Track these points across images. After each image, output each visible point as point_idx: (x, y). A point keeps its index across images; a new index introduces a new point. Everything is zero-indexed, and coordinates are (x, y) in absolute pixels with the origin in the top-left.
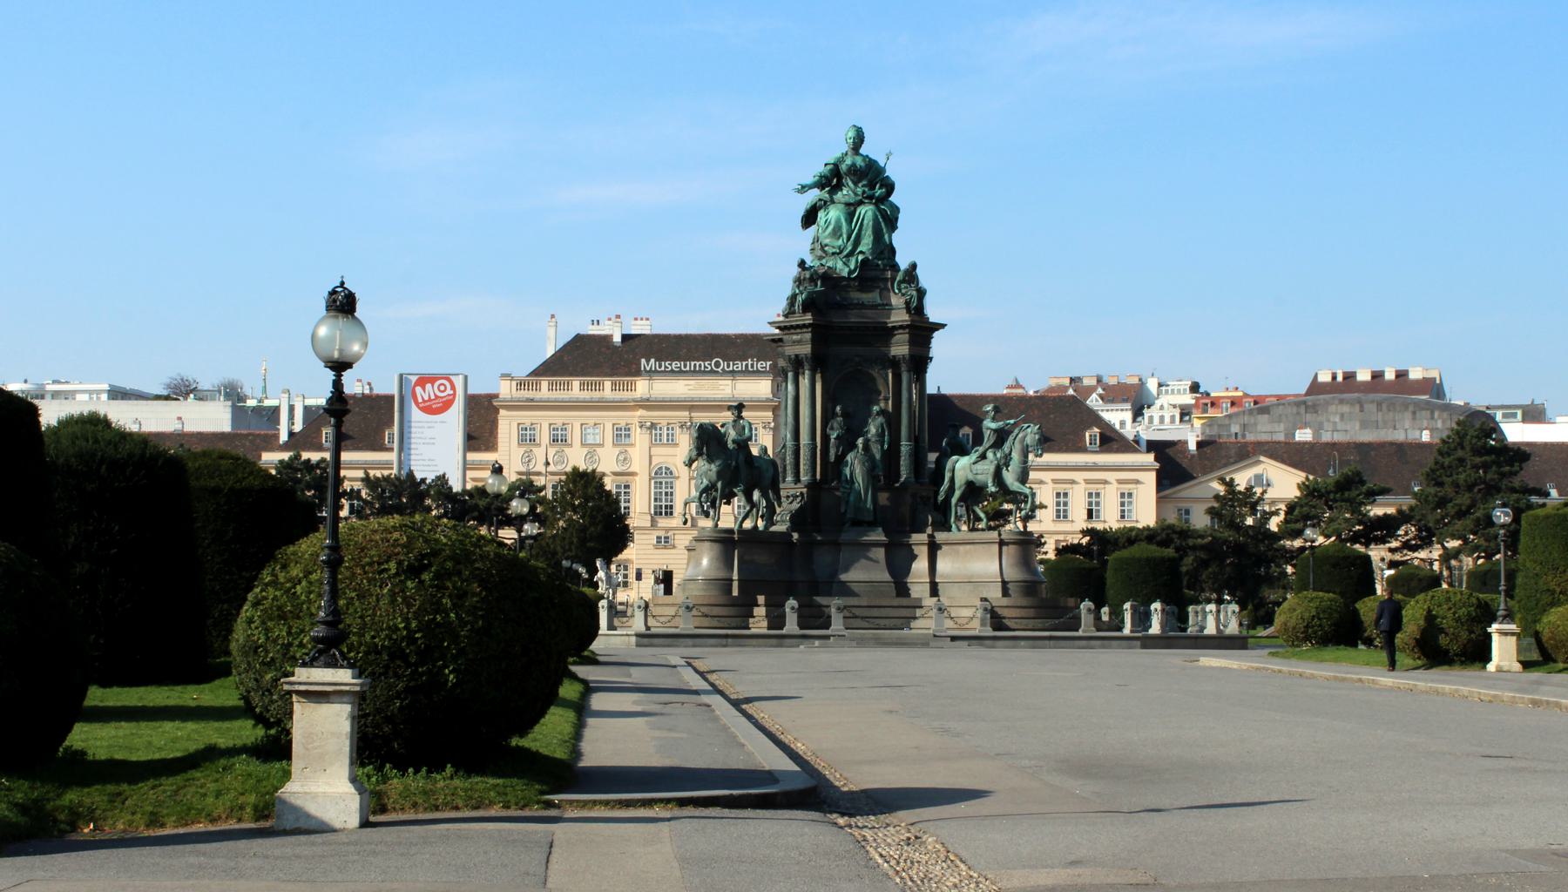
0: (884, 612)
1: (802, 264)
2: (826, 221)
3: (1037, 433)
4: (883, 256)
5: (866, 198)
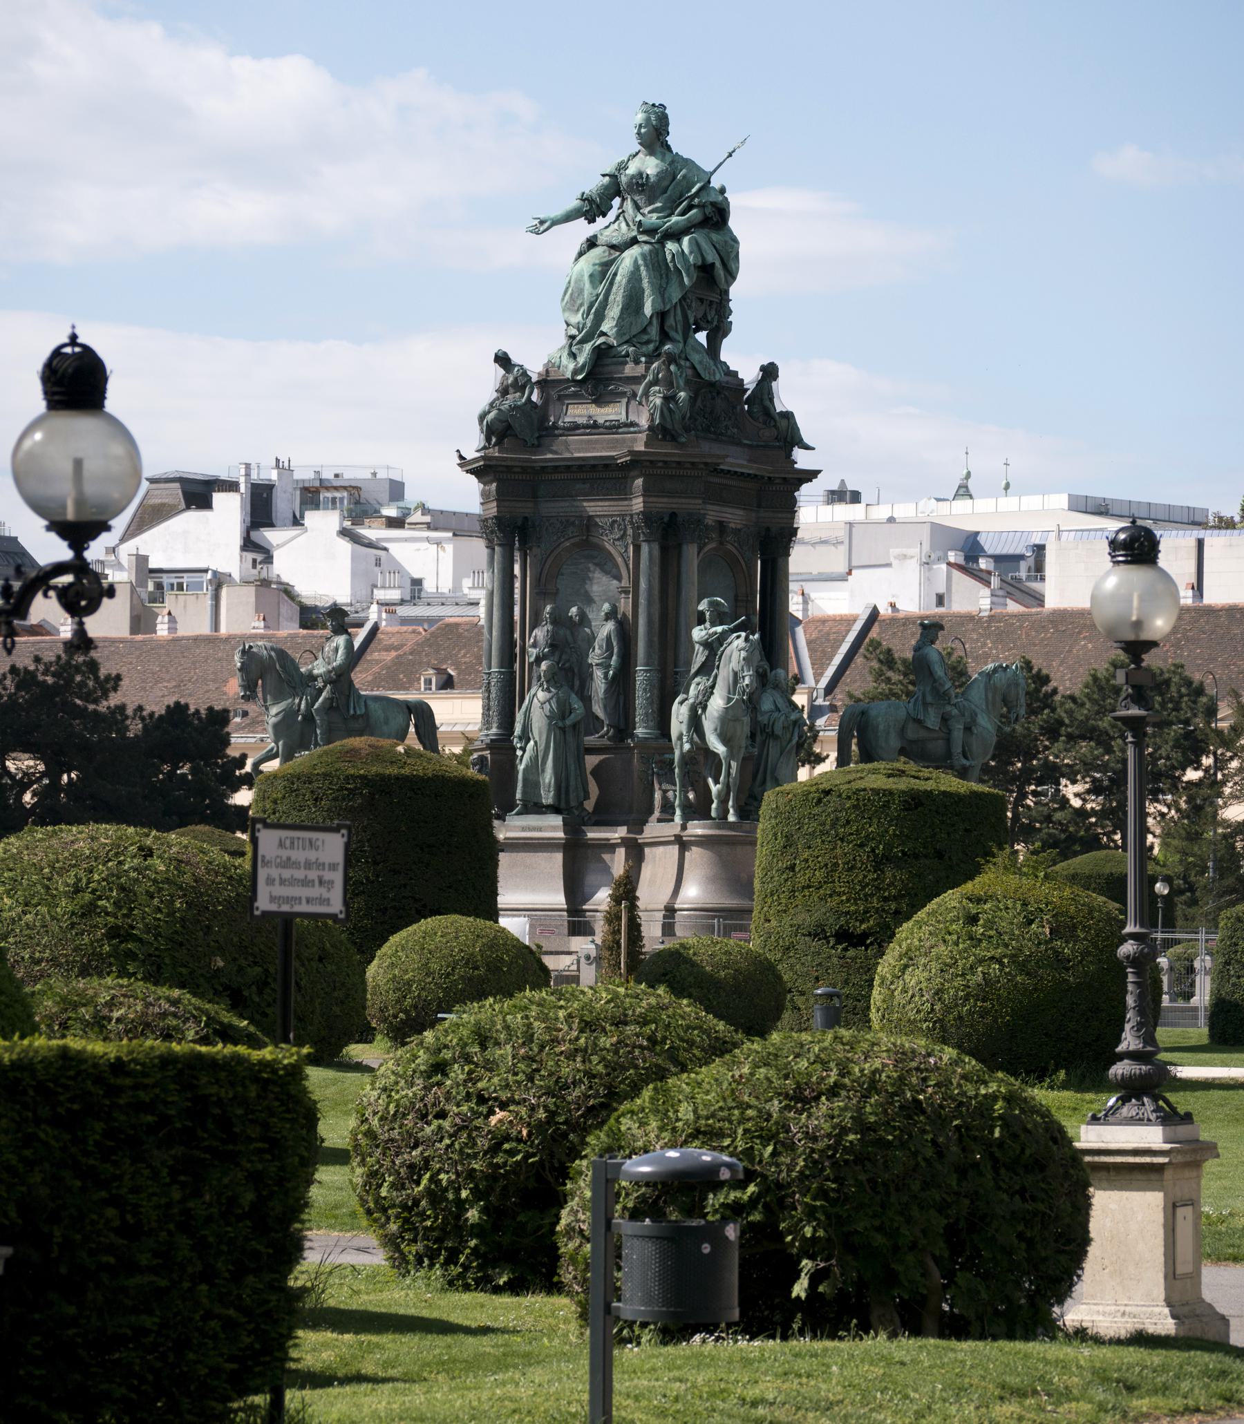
1: (503, 360)
4: (645, 338)
5: (645, 232)
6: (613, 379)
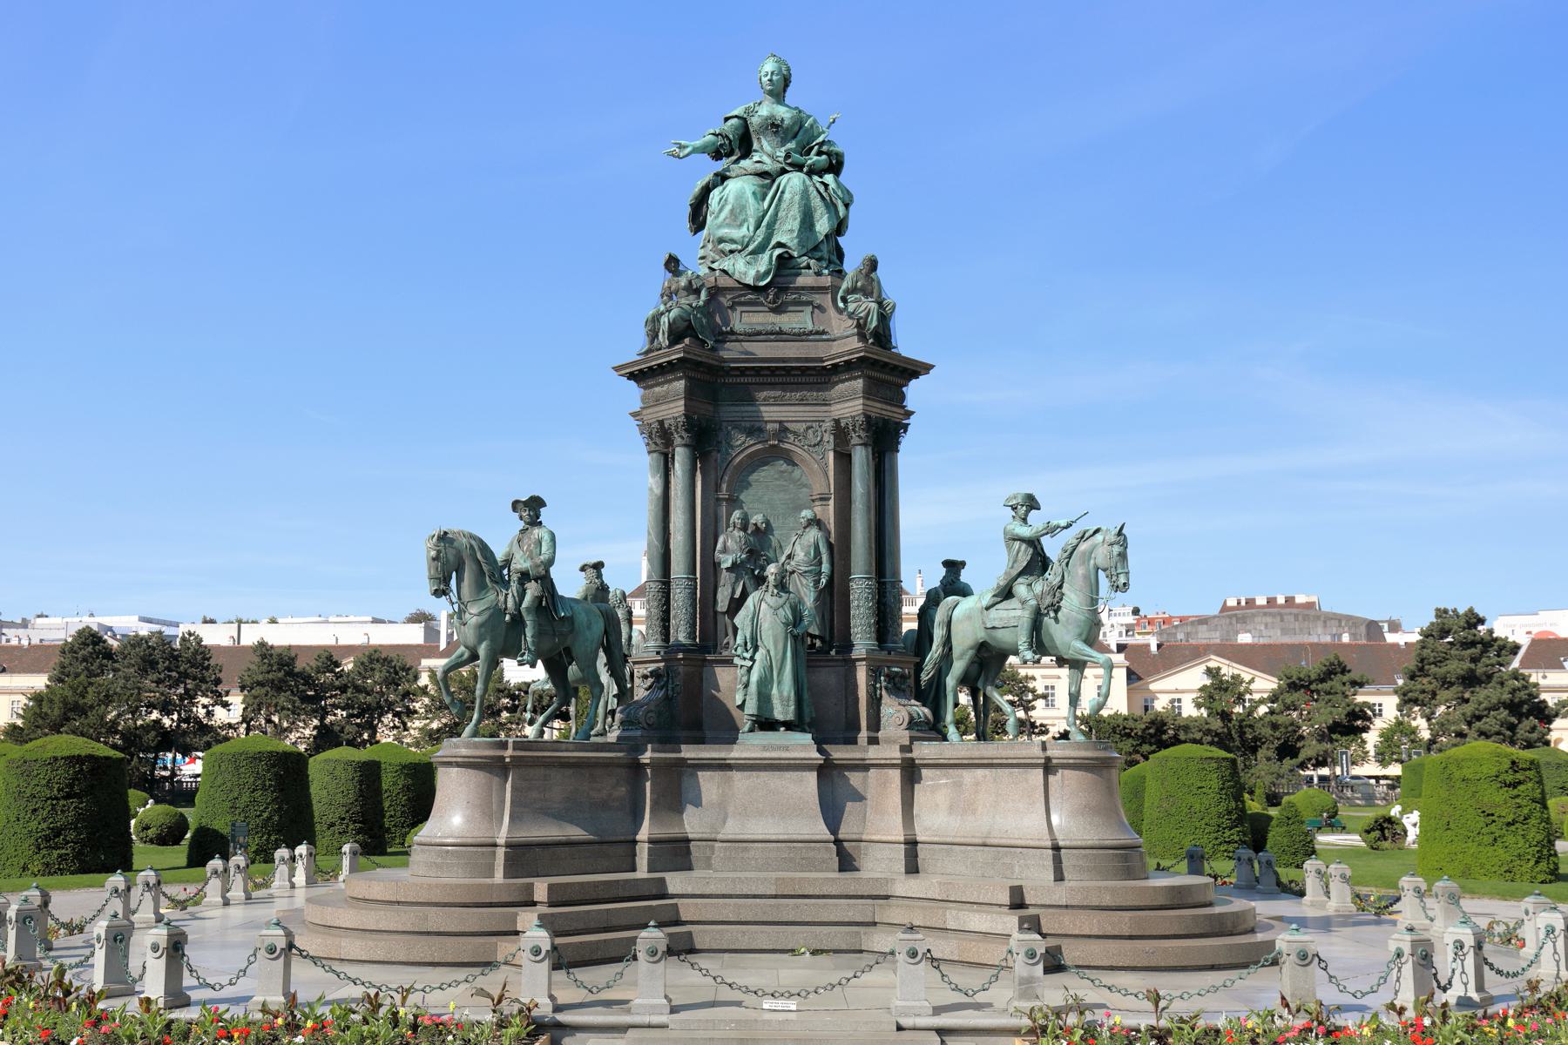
0: (807, 910)
1: (673, 264)
2: (721, 199)
3: (1118, 543)
4: (818, 254)
5: (790, 164)
6: (787, 288)
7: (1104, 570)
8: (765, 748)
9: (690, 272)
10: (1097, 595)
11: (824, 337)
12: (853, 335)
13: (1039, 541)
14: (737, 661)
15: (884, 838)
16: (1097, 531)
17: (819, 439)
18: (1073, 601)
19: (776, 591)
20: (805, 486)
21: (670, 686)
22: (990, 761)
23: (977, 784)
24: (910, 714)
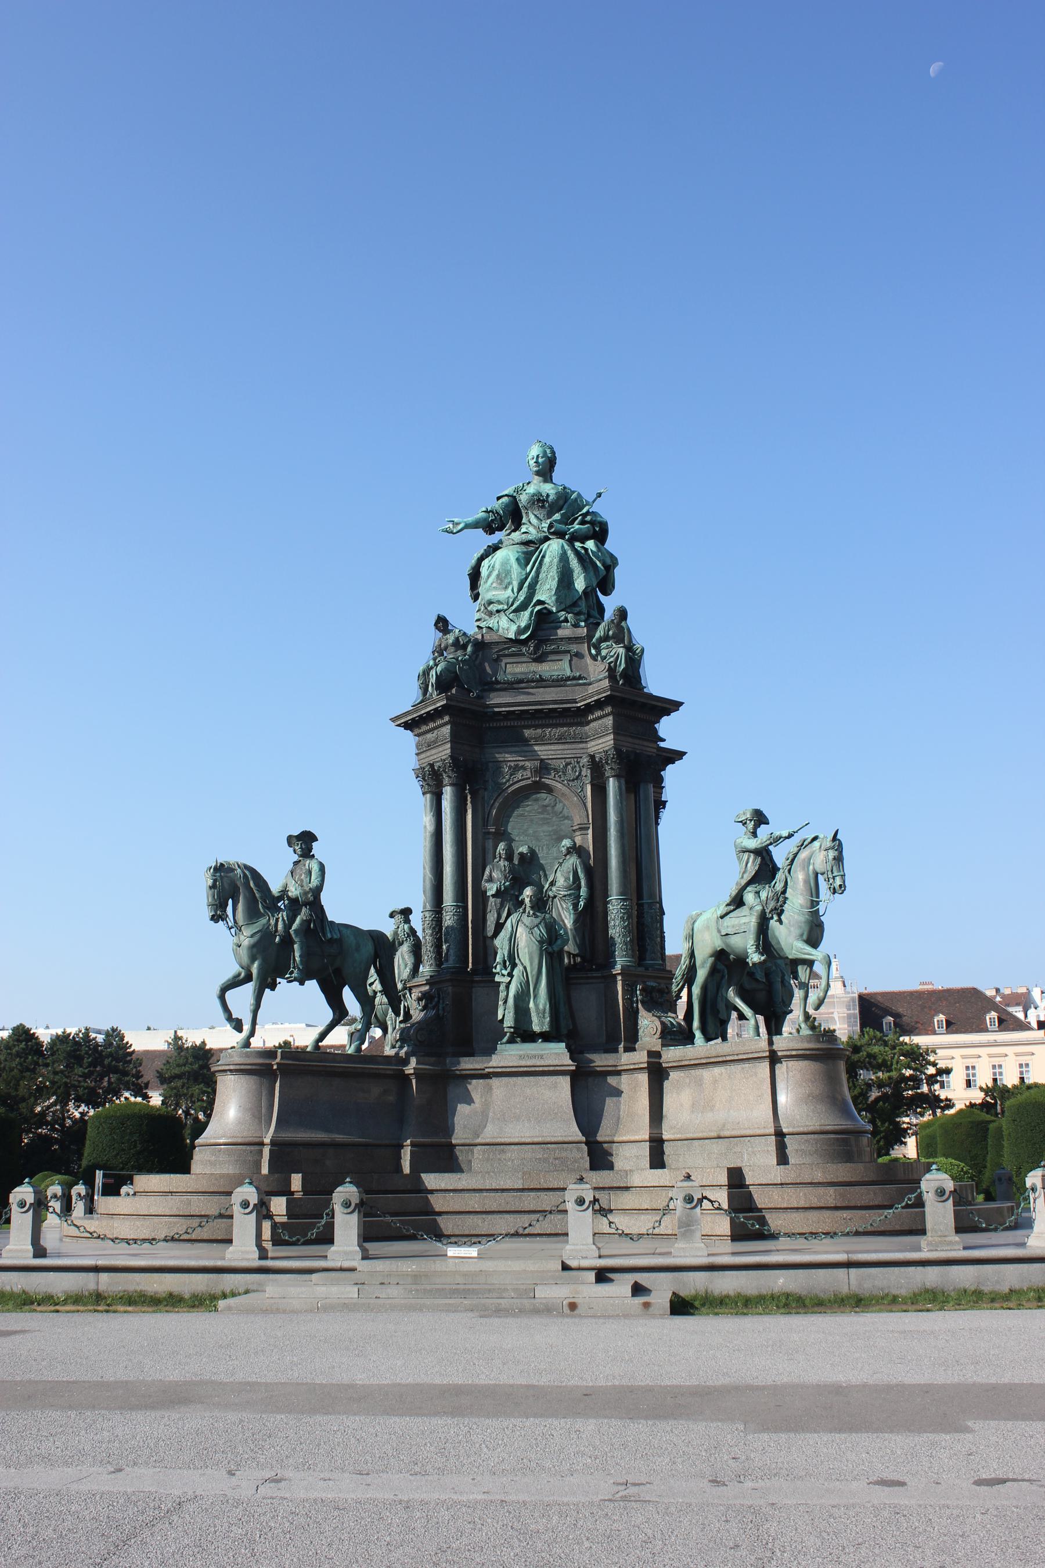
1: (442, 624)
2: (489, 567)
3: (833, 848)
4: (577, 610)
6: (548, 640)
7: (822, 874)
8: (521, 1057)
9: (457, 631)
10: (818, 896)
11: (581, 682)
12: (605, 678)
13: (769, 853)
14: (497, 979)
15: (632, 1138)
16: (815, 838)
17: (577, 773)
18: (796, 902)
19: (531, 912)
20: (567, 818)
21: (441, 1006)
22: (724, 1059)
23: (715, 1081)
24: (662, 1023)
